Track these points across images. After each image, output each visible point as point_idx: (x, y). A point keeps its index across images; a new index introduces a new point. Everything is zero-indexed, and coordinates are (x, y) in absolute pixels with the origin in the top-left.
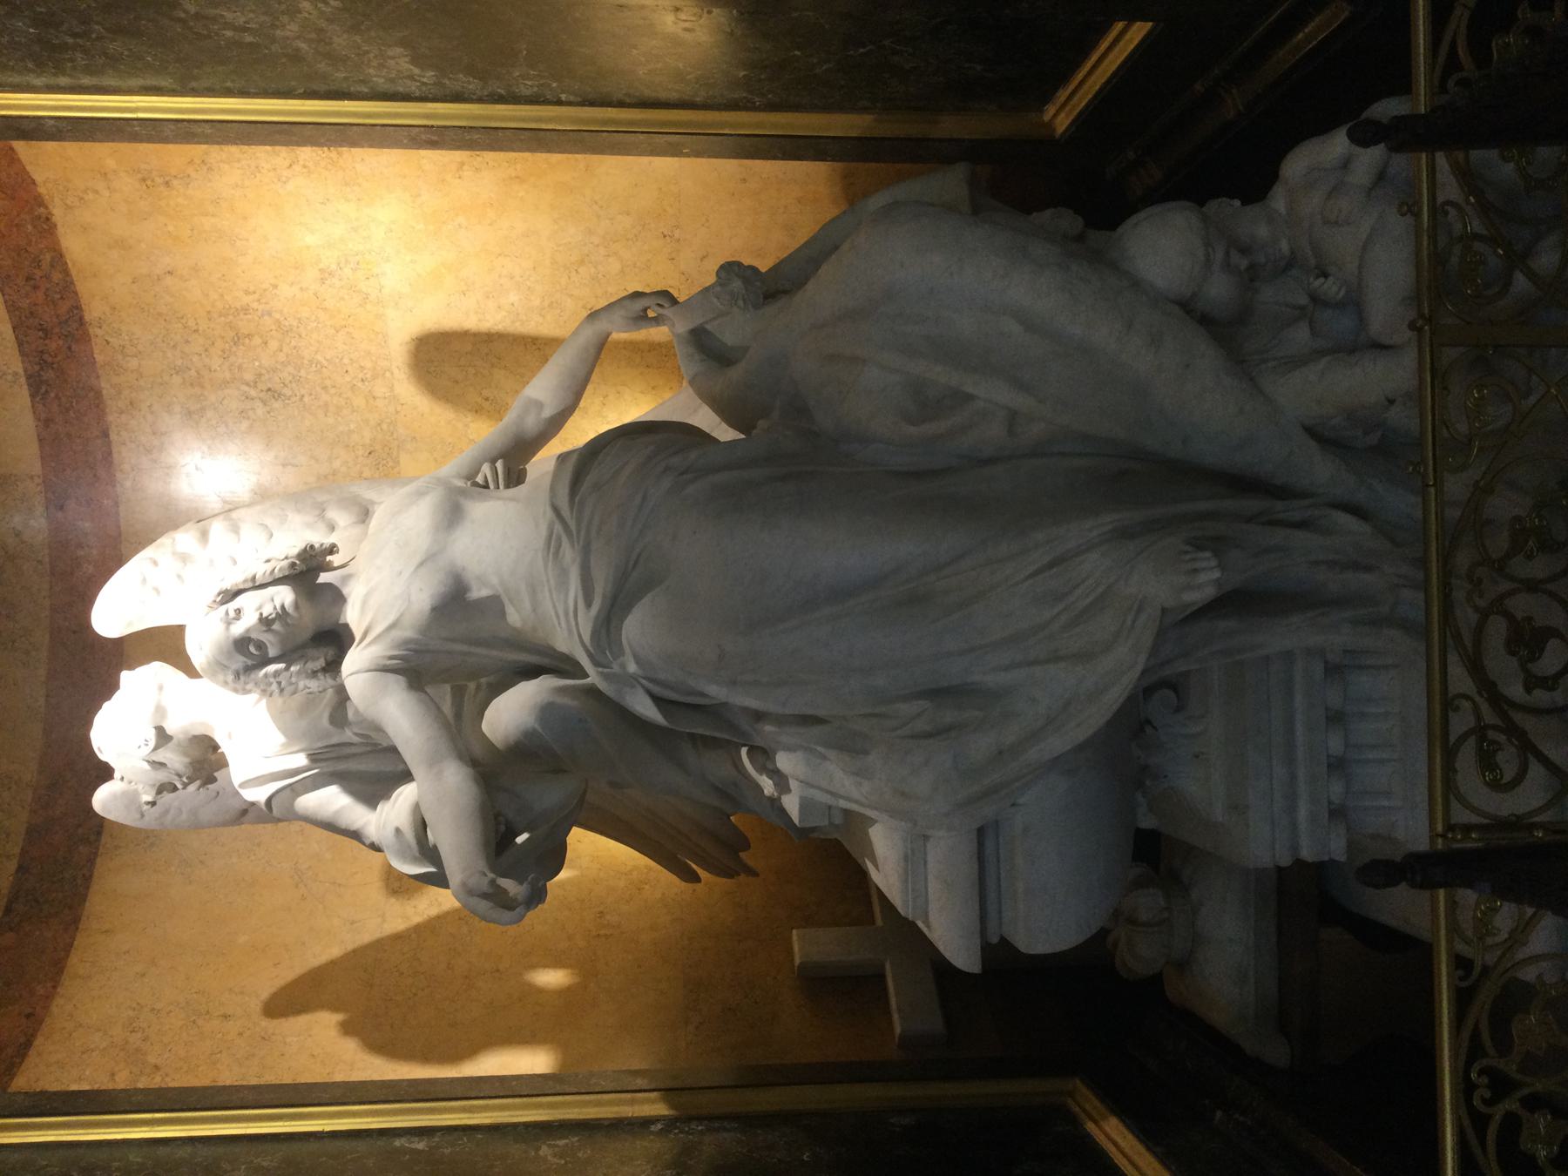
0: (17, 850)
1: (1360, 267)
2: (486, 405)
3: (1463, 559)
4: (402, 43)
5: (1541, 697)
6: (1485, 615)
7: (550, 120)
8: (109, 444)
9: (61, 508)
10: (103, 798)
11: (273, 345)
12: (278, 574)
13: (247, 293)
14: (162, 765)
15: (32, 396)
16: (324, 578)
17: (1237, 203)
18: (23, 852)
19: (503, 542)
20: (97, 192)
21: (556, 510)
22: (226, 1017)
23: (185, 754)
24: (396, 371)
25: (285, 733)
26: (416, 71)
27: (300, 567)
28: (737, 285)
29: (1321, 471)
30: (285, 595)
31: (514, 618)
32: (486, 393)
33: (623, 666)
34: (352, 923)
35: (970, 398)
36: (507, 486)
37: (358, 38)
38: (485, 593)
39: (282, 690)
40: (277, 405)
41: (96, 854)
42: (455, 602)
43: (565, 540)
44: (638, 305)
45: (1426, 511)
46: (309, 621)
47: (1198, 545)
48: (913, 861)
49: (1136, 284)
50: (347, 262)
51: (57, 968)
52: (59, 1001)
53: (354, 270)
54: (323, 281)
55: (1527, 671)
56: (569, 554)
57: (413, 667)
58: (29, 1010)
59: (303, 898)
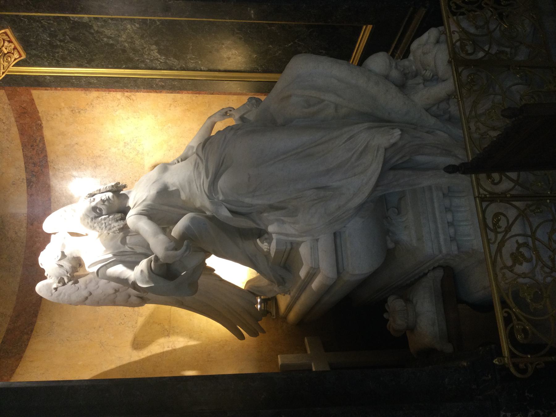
1: (435, 63)
4: (157, 44)
7: (197, 76)
10: (40, 288)
12: (108, 189)
13: (101, 151)
14: (62, 266)
15: (28, 186)
18: (4, 337)
20: (57, 115)
23: (70, 263)
25: (105, 247)
26: (159, 56)
27: (115, 189)
28: (254, 101)
31: (183, 196)
33: (218, 198)
34: (120, 358)
35: (323, 101)
37: (143, 41)
38: (174, 189)
39: (106, 227)
41: (30, 338)
42: (164, 193)
43: (200, 162)
44: (224, 111)
45: (464, 134)
46: (117, 203)
50: (133, 140)
53: (135, 143)
54: (125, 146)
57: (150, 213)
59: (103, 350)
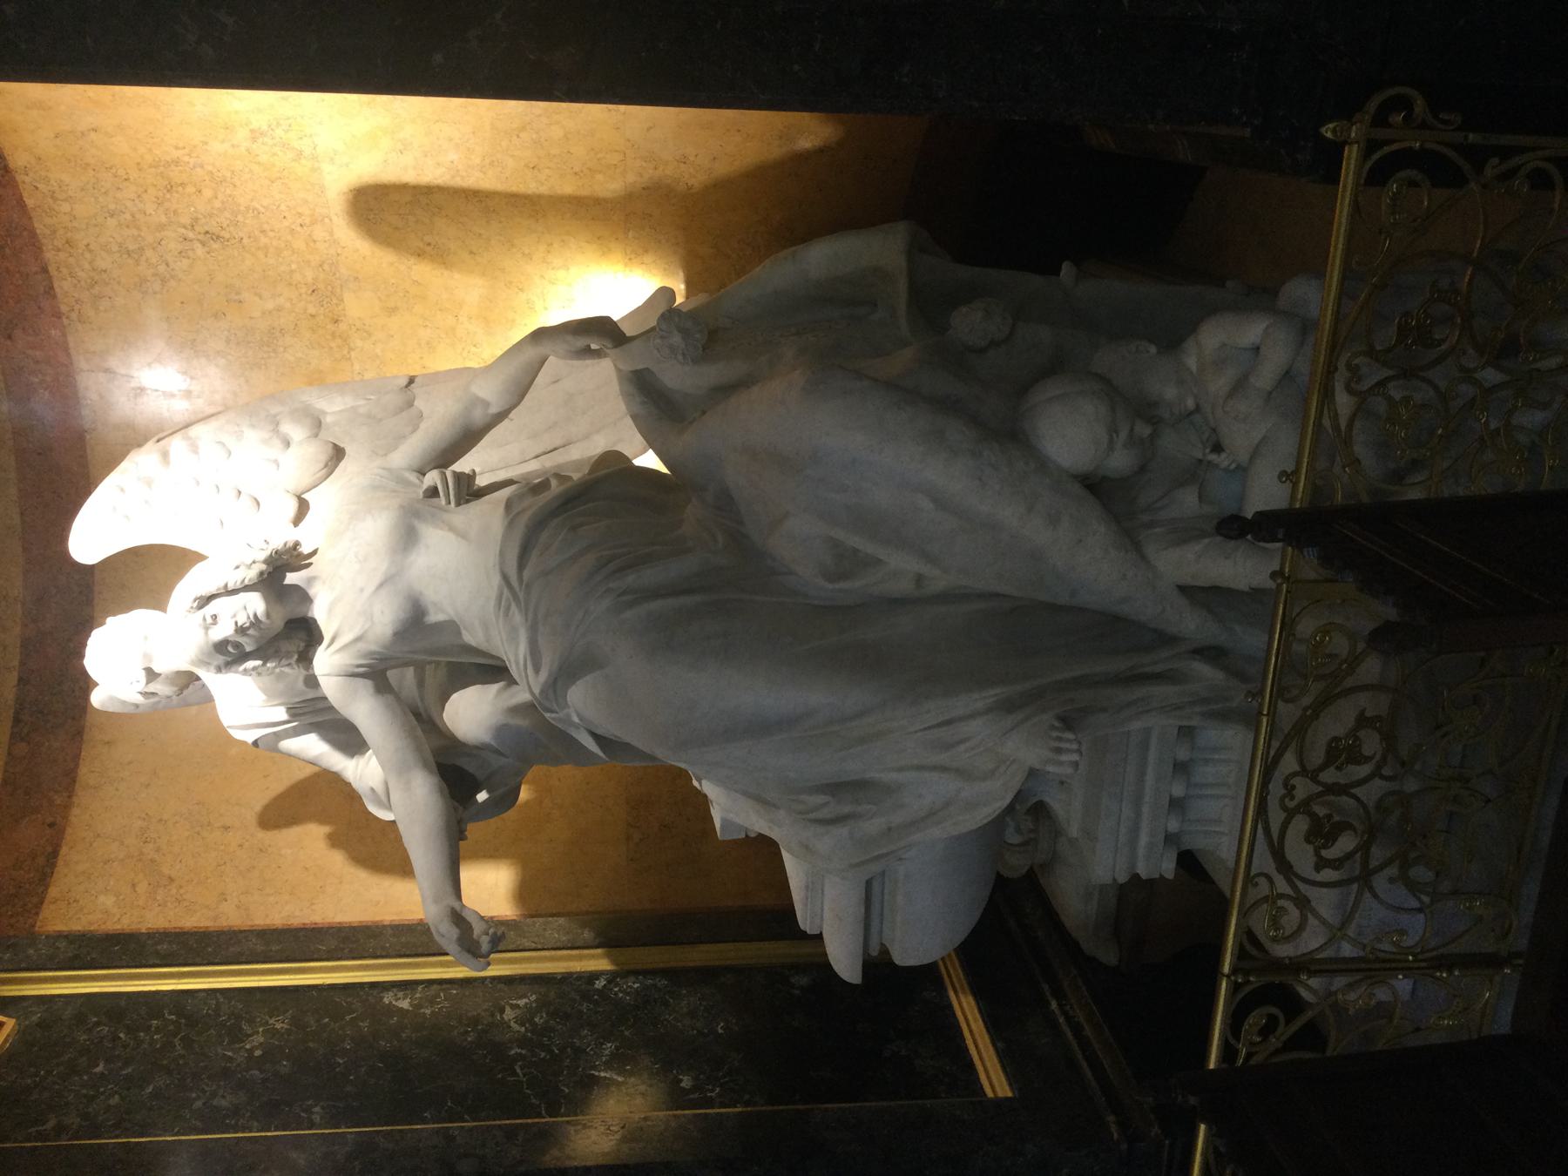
0: (16, 663)
2: (428, 249)
3: (1289, 763)
5: (1328, 875)
6: (1291, 814)
8: (50, 278)
9: (10, 337)
11: (207, 193)
13: (177, 148)
16: (291, 578)
17: (1153, 349)
18: (22, 663)
19: (458, 568)
21: (505, 577)
22: (226, 828)
24: (335, 218)
29: (1192, 624)
30: (255, 604)
32: (427, 238)
35: (879, 561)
36: (458, 504)
40: (215, 246)
43: (514, 607)
47: (1067, 723)
48: (814, 888)
49: (1043, 465)
50: (278, 124)
51: (69, 778)
52: (75, 811)
53: (287, 131)
54: (254, 140)
55: (1317, 853)
56: (517, 617)
58: (50, 819)
